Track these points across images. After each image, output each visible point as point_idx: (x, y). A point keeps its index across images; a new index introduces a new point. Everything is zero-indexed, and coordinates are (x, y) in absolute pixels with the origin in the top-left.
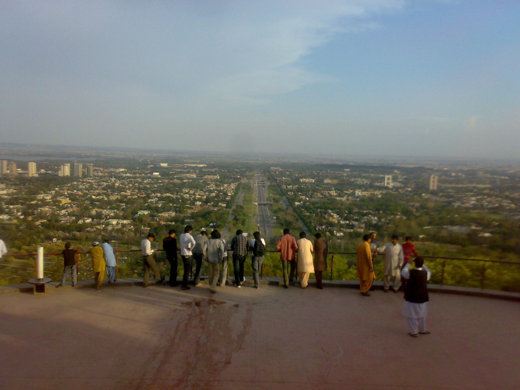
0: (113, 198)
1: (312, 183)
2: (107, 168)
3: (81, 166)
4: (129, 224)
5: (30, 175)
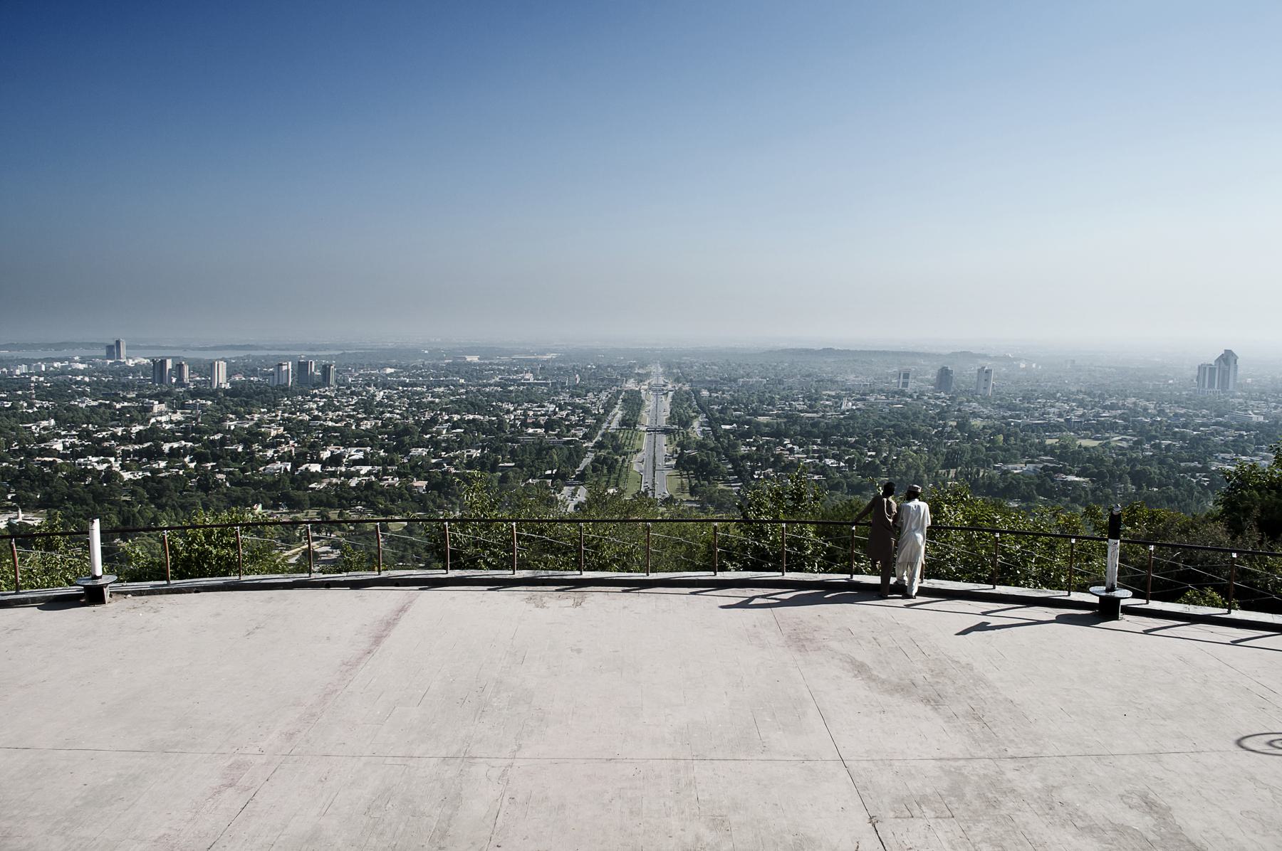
0: (367, 425)
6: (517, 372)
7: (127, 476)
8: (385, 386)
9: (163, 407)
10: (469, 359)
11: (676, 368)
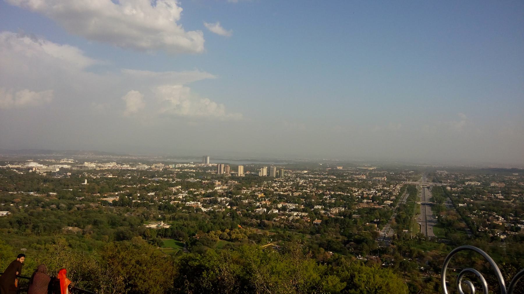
0: (296, 194)
1: (478, 186)
2: (294, 170)
3: (275, 169)
4: (306, 216)
5: (239, 175)
6: (359, 175)
7: (204, 210)
8: (305, 178)
9: (220, 183)
10: (338, 168)
11: (432, 175)
